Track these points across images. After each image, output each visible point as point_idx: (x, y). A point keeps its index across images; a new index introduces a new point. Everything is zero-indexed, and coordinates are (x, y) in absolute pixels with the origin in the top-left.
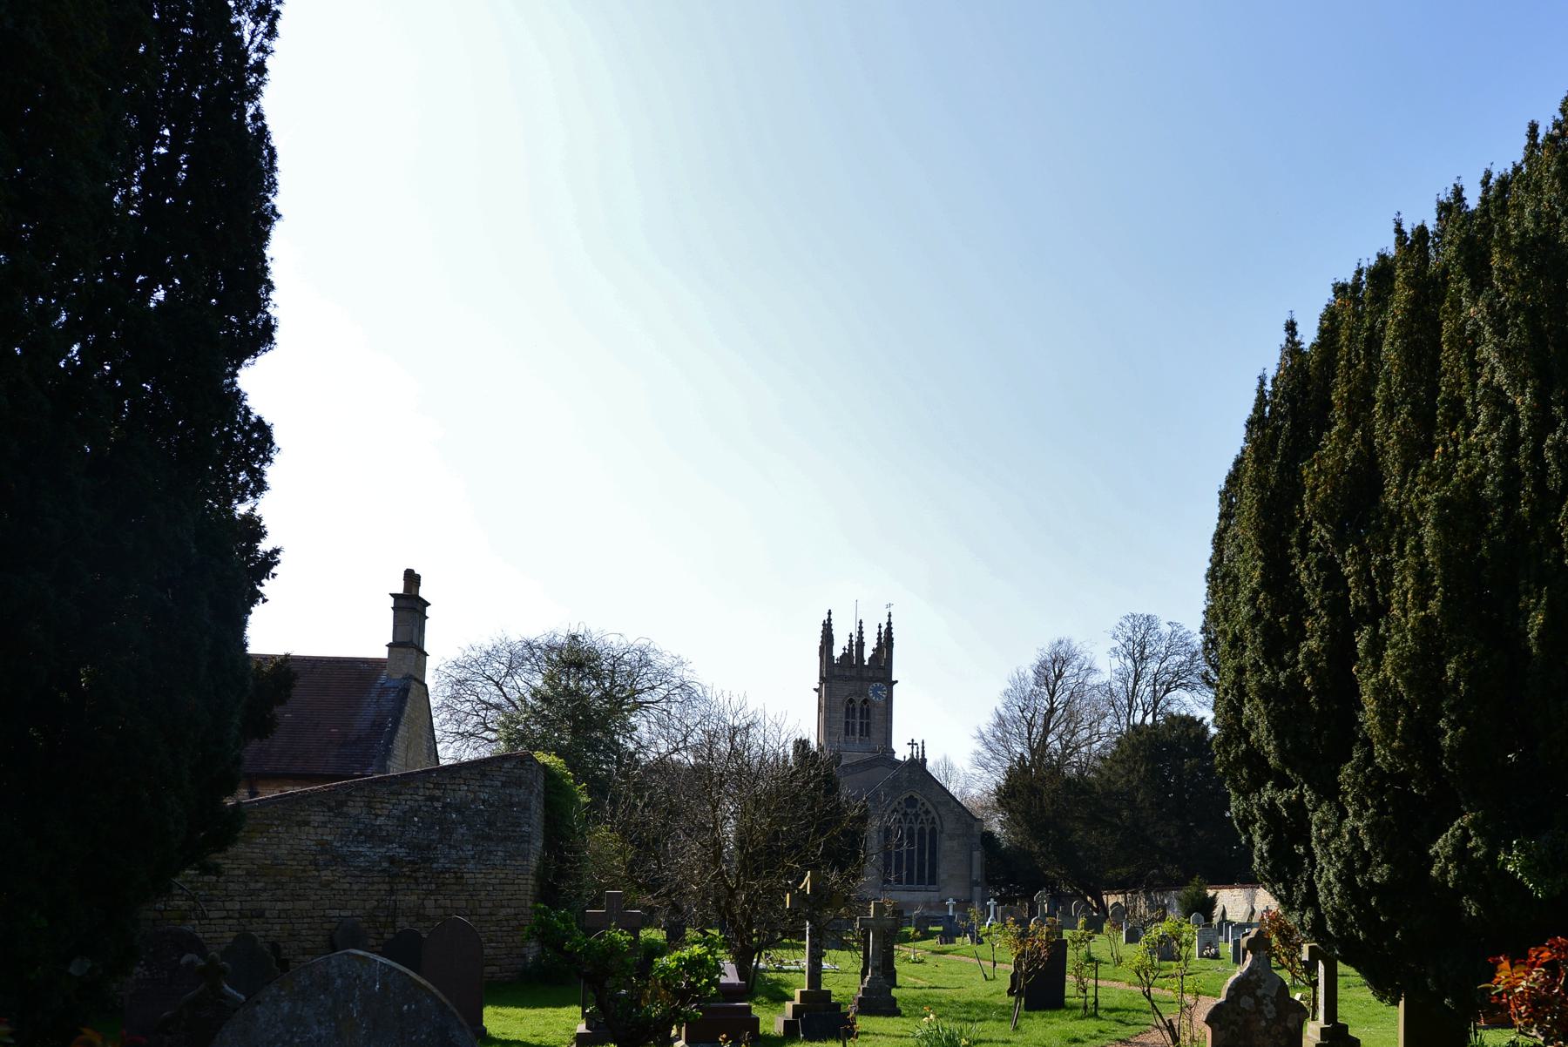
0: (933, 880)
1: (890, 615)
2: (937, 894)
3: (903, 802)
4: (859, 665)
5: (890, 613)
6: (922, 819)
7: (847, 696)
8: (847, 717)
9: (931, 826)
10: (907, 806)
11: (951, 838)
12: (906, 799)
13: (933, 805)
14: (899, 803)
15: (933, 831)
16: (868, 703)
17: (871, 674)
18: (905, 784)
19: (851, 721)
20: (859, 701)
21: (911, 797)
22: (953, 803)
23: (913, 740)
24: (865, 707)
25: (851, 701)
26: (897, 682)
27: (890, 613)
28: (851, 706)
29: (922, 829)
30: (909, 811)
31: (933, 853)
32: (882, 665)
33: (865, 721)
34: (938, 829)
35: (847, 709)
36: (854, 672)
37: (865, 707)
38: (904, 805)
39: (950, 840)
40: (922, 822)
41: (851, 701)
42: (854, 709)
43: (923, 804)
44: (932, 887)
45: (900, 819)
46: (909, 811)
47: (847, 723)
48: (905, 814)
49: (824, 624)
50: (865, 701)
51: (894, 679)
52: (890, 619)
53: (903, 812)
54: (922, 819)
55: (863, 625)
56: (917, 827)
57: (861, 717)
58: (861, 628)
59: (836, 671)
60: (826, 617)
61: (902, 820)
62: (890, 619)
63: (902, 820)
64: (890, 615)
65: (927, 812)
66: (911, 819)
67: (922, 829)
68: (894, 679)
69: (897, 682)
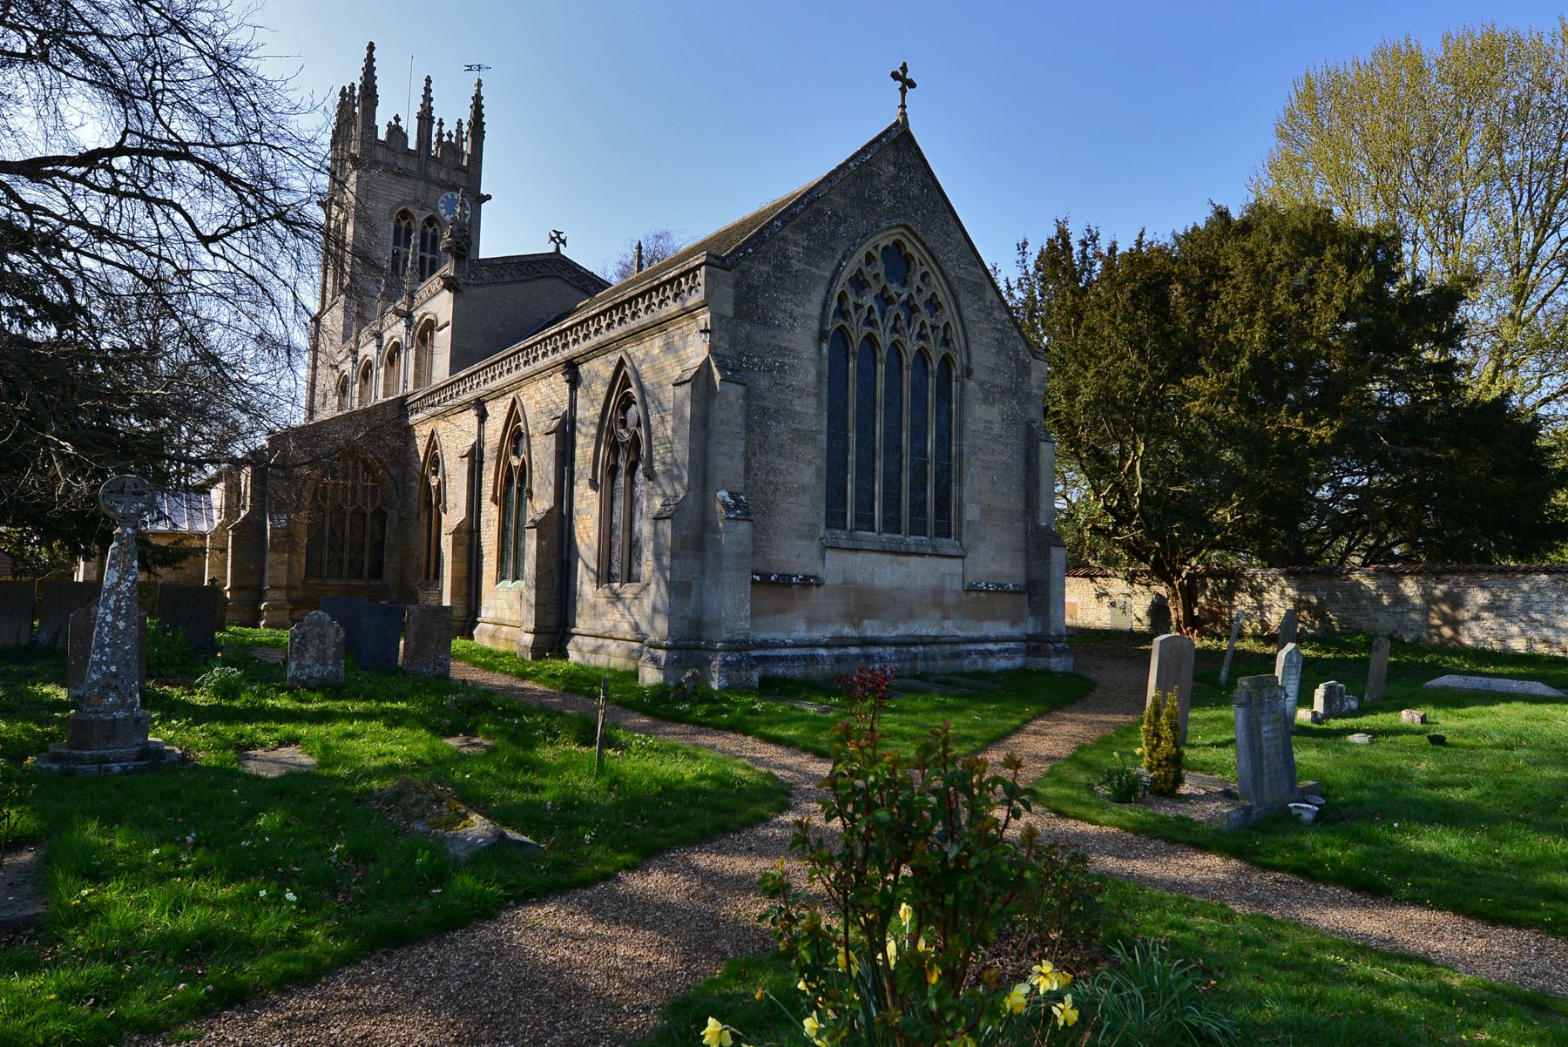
0: (944, 530)
1: (479, 84)
2: (955, 566)
3: (877, 255)
4: (423, 152)
5: (480, 80)
6: (923, 324)
7: (399, 204)
8: (396, 242)
9: (944, 350)
10: (892, 275)
11: (988, 399)
12: (886, 248)
13: (949, 285)
14: (870, 258)
15: (946, 361)
16: (436, 226)
17: (443, 175)
18: (888, 202)
19: (402, 249)
20: (420, 217)
21: (898, 244)
22: (990, 295)
23: (904, 68)
24: (430, 231)
25: (405, 214)
26: (489, 197)
27: (480, 80)
28: (404, 224)
29: (922, 354)
30: (894, 288)
31: (944, 440)
32: (465, 164)
33: (429, 256)
34: (958, 360)
35: (397, 230)
36: (412, 165)
37: (430, 231)
38: (880, 268)
39: (986, 401)
40: (921, 337)
41: (405, 214)
42: (409, 232)
43: (924, 276)
44: (946, 545)
45: (871, 309)
46: (894, 288)
47: (396, 256)
48: (885, 299)
49: (343, 93)
50: (431, 221)
51: (484, 191)
52: (479, 91)
53: (876, 289)
54: (923, 324)
55: (432, 86)
56: (911, 346)
57: (423, 247)
58: (428, 90)
59: (380, 154)
60: (355, 77)
61: (877, 315)
62: (479, 91)
63: (877, 315)
64: (479, 84)
65: (934, 305)
66: (897, 317)
67: (922, 354)
68: (484, 191)
69: (489, 197)
